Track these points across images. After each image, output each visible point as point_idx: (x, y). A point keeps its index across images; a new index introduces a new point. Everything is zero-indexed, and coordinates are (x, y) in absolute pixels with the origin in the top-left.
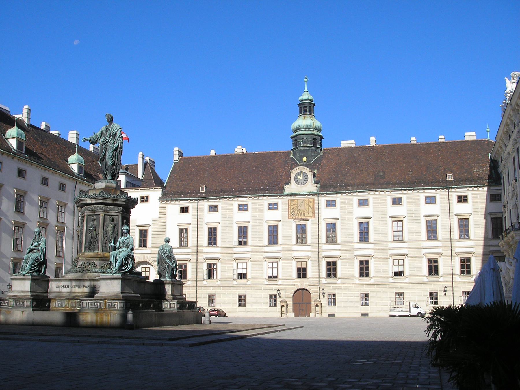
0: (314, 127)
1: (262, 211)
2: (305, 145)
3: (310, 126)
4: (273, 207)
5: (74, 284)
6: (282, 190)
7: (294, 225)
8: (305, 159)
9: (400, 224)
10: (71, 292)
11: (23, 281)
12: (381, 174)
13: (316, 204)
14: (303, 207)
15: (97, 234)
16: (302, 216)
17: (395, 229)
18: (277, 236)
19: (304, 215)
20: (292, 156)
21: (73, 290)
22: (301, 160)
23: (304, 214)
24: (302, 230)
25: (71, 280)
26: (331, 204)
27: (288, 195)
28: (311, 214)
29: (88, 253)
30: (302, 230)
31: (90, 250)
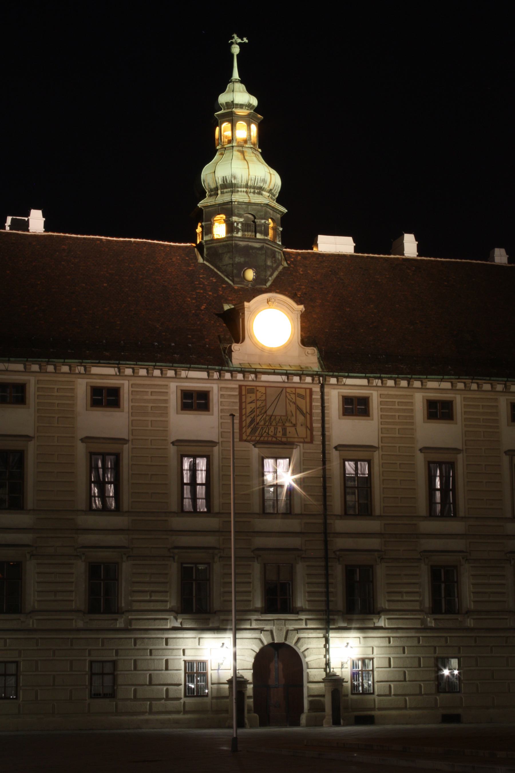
0: (271, 187)
2: (248, 234)
3: (264, 181)
4: (195, 401)
16: (279, 434)
19: (284, 434)
23: (284, 430)
28: (302, 431)
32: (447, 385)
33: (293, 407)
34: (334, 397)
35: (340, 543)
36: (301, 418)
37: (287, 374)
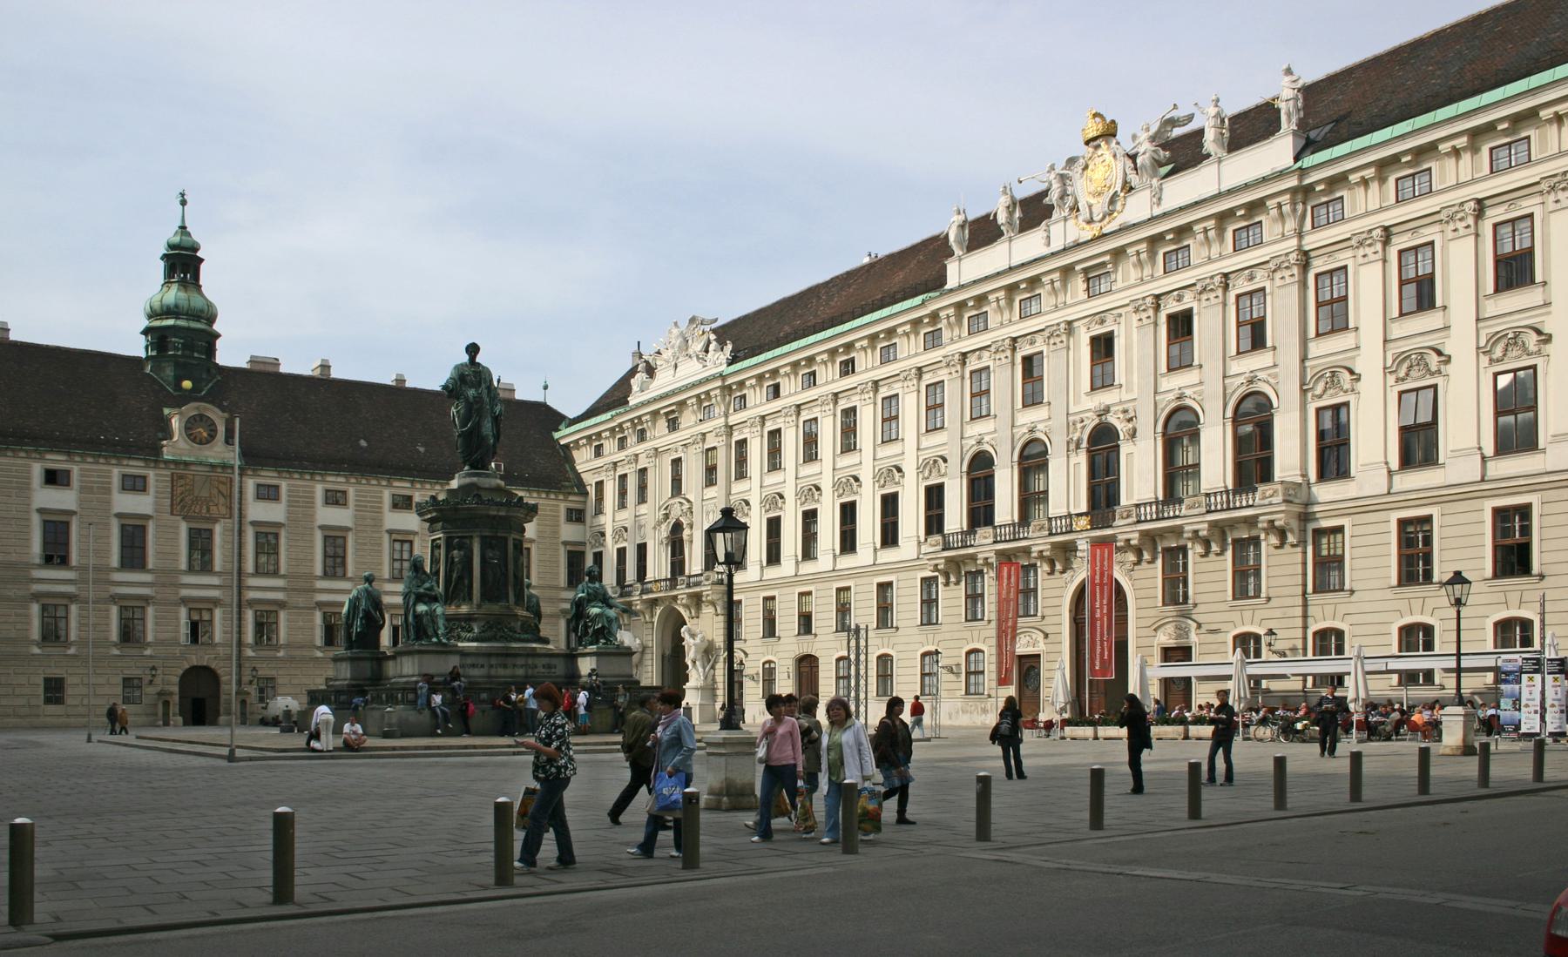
1: (108, 491)
4: (134, 484)
5: (494, 661)
6: (157, 451)
7: (183, 528)
8: (187, 384)
9: (406, 546)
10: (489, 677)
11: (443, 657)
12: (363, 443)
13: (236, 490)
14: (205, 494)
15: (505, 575)
17: (397, 556)
18: (143, 548)
20: (148, 369)
21: (493, 672)
22: (178, 386)
24: (200, 544)
25: (489, 655)
26: (268, 494)
27: (175, 462)
28: (223, 510)
29: (495, 608)
30: (200, 544)
31: (490, 600)
32: (342, 479)
33: (215, 491)
34: (250, 485)
35: (252, 595)
36: (222, 500)
37: (213, 466)
